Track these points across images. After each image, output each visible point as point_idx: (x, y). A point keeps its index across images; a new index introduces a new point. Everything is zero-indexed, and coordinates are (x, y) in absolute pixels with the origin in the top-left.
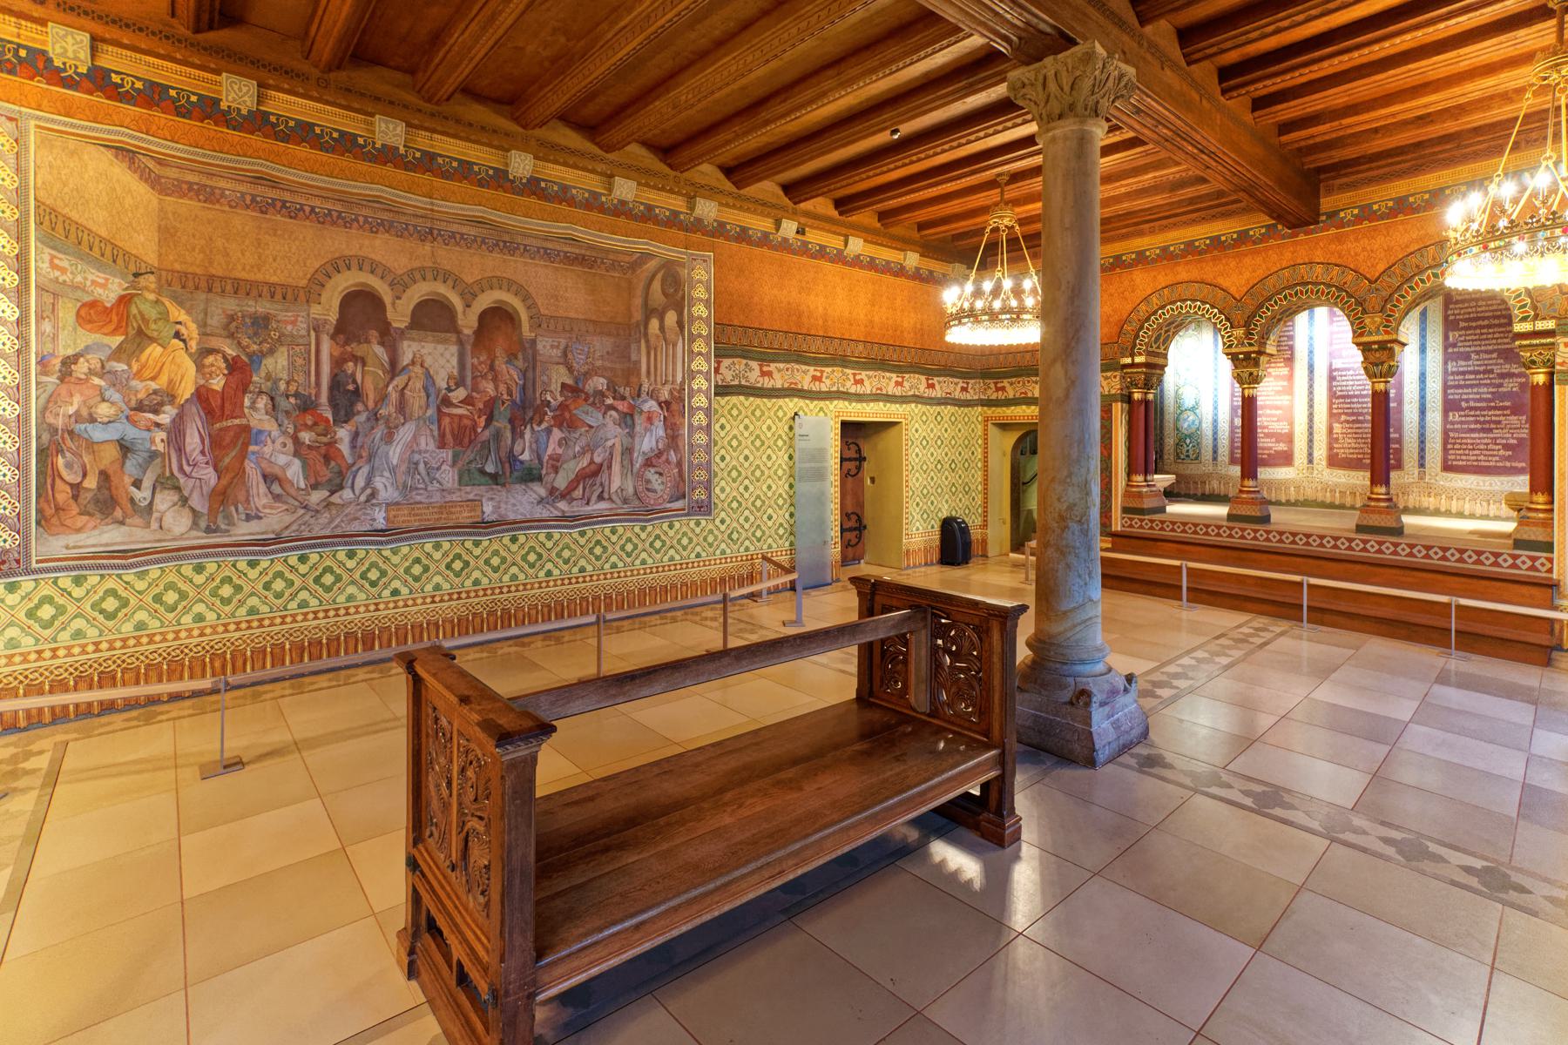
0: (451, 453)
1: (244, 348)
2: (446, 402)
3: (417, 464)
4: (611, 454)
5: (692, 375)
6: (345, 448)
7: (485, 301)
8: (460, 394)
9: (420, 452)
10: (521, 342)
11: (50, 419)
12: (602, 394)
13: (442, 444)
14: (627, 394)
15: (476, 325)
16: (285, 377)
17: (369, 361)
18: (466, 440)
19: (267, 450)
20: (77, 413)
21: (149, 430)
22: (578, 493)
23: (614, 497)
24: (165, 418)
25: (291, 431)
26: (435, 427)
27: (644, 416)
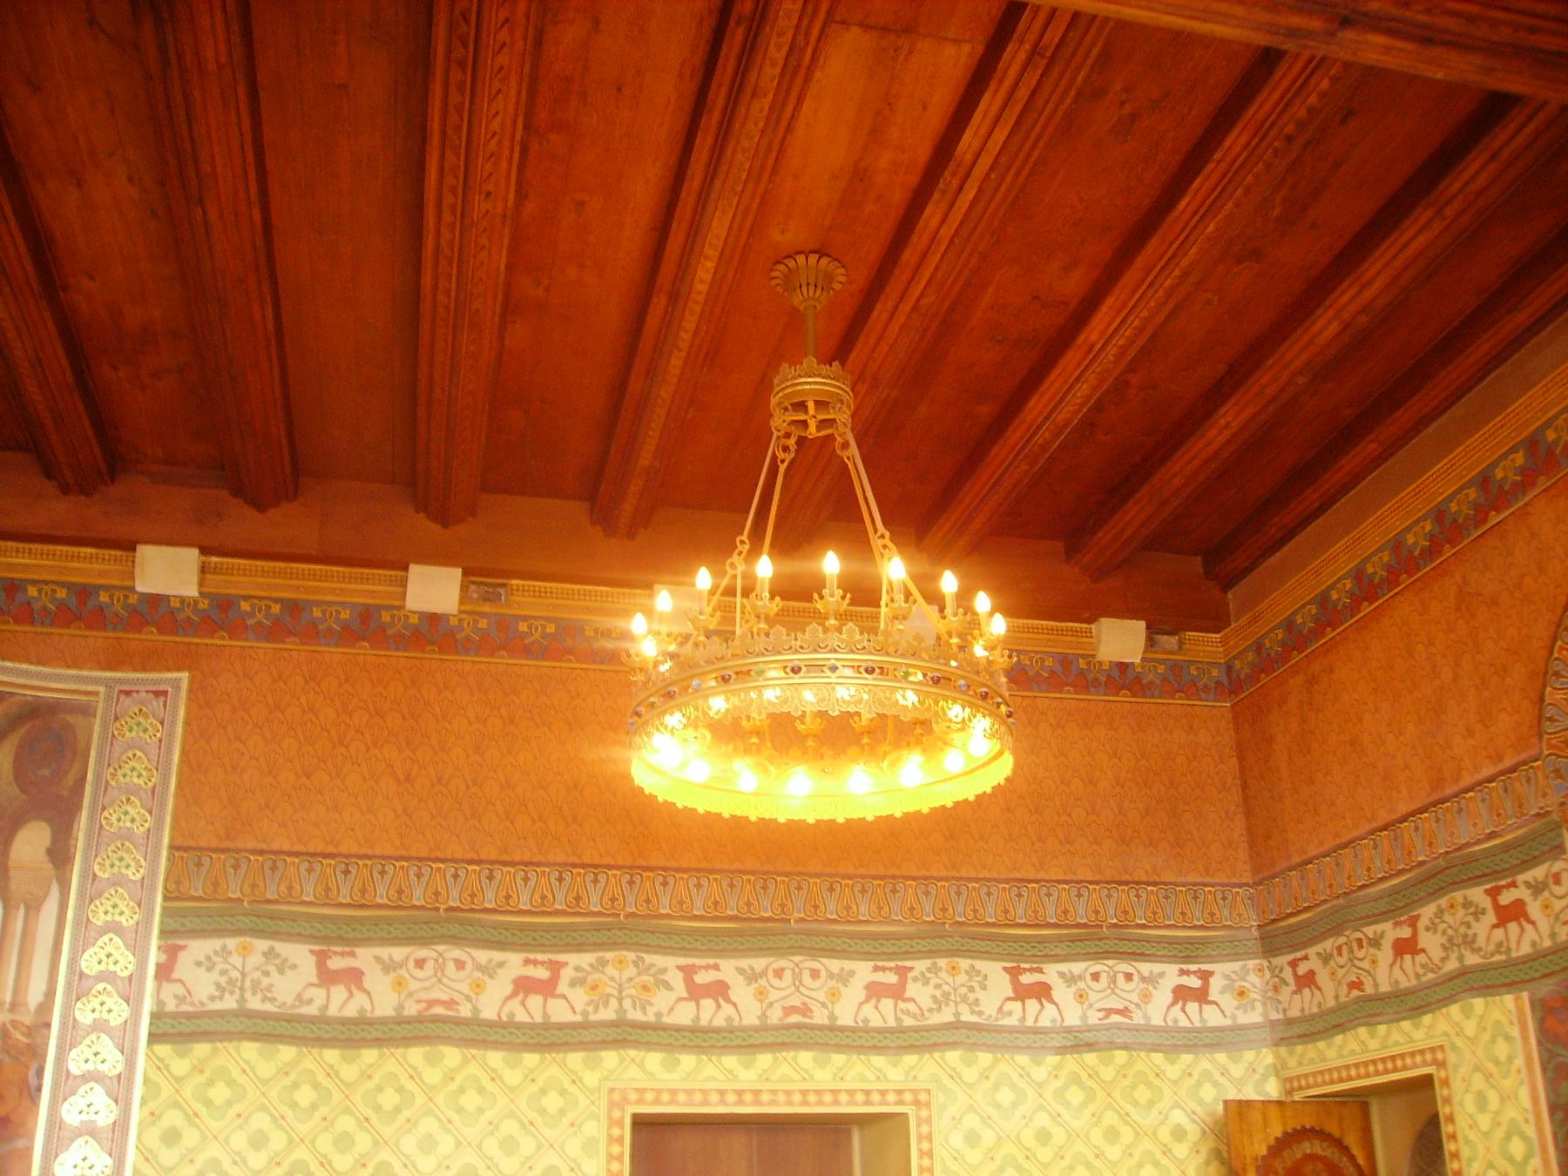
5: (80, 986)
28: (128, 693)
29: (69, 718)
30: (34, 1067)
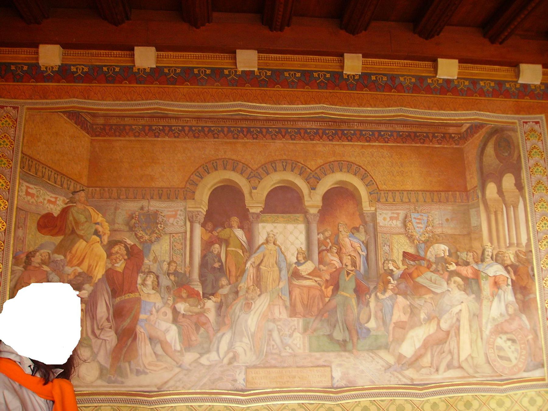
1: (139, 238)
2: (296, 275)
3: (270, 331)
4: (458, 320)
6: (212, 316)
7: (328, 183)
8: (307, 268)
9: (274, 320)
10: (362, 215)
12: (443, 261)
13: (293, 313)
14: (471, 260)
15: (320, 204)
16: (168, 259)
17: (232, 241)
18: (315, 310)
22: (426, 360)
23: (464, 365)
25: (171, 302)
26: (287, 298)
27: (491, 281)
28: (526, 123)
29: (509, 133)
30: (530, 267)
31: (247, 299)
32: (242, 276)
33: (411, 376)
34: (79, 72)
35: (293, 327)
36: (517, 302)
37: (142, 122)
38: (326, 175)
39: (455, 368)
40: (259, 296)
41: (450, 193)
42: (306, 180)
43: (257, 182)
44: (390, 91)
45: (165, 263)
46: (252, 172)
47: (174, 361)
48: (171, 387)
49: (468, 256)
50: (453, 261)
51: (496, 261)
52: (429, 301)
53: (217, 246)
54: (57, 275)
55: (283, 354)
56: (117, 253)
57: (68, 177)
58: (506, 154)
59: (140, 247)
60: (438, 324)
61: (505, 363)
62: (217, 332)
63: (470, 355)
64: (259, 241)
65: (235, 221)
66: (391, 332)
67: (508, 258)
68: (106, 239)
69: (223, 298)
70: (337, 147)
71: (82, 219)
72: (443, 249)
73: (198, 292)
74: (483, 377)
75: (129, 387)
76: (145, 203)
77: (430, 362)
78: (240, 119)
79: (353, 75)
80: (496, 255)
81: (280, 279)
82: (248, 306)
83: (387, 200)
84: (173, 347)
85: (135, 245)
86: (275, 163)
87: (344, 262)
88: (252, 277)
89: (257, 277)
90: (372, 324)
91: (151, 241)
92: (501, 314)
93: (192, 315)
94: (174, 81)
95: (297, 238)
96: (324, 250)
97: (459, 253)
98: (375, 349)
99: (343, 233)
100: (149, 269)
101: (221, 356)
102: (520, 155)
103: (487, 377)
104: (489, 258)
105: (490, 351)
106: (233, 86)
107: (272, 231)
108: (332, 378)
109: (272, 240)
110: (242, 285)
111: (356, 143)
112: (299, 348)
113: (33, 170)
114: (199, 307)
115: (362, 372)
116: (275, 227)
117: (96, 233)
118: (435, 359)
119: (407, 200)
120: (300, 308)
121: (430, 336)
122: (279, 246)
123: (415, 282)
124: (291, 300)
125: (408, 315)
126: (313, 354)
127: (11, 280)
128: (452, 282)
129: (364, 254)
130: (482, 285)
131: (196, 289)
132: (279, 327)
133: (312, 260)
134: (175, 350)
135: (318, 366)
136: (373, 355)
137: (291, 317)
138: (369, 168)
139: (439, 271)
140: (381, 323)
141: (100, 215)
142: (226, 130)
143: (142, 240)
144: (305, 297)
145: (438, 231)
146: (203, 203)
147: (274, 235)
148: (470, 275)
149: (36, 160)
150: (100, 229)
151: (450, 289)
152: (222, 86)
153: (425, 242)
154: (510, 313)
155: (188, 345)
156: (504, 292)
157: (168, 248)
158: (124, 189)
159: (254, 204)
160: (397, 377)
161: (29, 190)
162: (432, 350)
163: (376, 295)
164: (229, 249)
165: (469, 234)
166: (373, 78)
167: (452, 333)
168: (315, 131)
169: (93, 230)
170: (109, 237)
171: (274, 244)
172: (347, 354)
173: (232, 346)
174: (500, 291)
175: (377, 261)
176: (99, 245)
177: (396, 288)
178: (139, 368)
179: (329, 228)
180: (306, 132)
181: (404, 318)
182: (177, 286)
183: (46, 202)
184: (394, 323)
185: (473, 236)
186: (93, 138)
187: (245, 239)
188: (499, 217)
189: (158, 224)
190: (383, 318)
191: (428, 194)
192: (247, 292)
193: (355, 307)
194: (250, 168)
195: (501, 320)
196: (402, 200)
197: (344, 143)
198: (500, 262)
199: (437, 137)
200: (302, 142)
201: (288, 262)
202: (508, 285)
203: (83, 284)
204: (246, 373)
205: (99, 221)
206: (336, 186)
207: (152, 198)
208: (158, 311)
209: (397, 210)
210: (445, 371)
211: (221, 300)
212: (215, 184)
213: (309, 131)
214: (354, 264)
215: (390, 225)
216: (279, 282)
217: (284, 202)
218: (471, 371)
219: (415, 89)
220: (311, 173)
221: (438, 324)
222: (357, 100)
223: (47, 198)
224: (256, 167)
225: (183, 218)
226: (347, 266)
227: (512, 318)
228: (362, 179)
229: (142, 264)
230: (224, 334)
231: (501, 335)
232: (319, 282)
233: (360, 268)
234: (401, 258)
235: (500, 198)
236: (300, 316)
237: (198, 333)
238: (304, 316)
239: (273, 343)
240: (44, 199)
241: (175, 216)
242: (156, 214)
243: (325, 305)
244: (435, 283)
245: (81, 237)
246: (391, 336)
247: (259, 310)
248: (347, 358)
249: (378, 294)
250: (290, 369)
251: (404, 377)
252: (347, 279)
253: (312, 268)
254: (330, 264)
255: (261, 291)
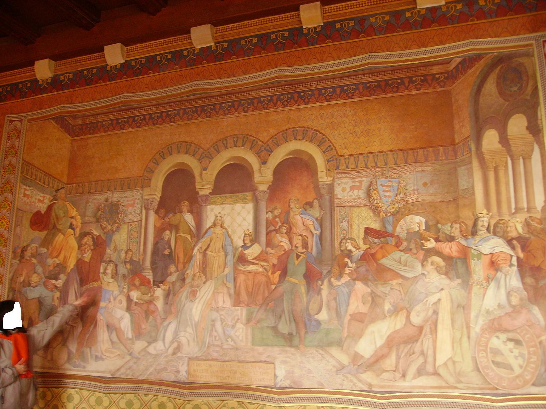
0: (245, 311)
1: (103, 229)
2: (242, 259)
4: (436, 312)
6: (160, 304)
7: (280, 155)
9: (217, 310)
10: (317, 188)
11: (13, 286)
12: (418, 238)
13: (237, 302)
14: (456, 233)
15: (271, 179)
18: (260, 298)
19: (110, 306)
20: (24, 281)
21: (52, 291)
22: (390, 362)
23: (441, 371)
24: (59, 283)
25: (125, 290)
26: (231, 285)
29: (520, 60)
31: (192, 286)
32: (189, 263)
33: (369, 380)
34: (66, 80)
35: (237, 318)
36: (526, 289)
37: (111, 117)
38: (278, 146)
39: (428, 374)
40: (204, 283)
41: (431, 149)
42: (257, 154)
43: (208, 162)
44: (358, 37)
45: (123, 252)
46: (203, 153)
47: (126, 348)
48: (122, 374)
49: (454, 229)
50: (432, 235)
51: (495, 234)
52: (397, 288)
53: (168, 232)
54: (41, 266)
55: (225, 346)
56: (86, 244)
57: (53, 177)
58: (515, 89)
59: (103, 237)
60: (408, 317)
61: (503, 372)
62: (164, 321)
63: (451, 358)
64: (206, 224)
65: (185, 204)
66: (346, 326)
67: (513, 228)
68: (78, 231)
69: (171, 286)
70: (292, 113)
71: (61, 213)
72: (418, 221)
73: (149, 279)
74: (468, 388)
75: (89, 371)
76: (109, 195)
77: (394, 365)
78: (195, 99)
79: (315, 28)
80: (495, 226)
81: (226, 264)
82: (194, 294)
83: (347, 167)
84: (126, 335)
85: (100, 235)
86: (226, 140)
87: (294, 243)
88: (198, 263)
89: (203, 263)
90: (323, 316)
91: (112, 230)
92: (499, 306)
93: (143, 303)
94: (140, 73)
95: (244, 219)
96: (272, 231)
97: (440, 226)
98: (325, 345)
99: (295, 210)
100: (110, 258)
101: (167, 346)
102: (537, 87)
103: (474, 388)
104: (484, 229)
105: (481, 355)
106: (191, 66)
107: (220, 213)
108: (275, 376)
109: (220, 222)
110: (188, 272)
111: (314, 105)
112: (242, 341)
113: (30, 174)
114: (149, 295)
115: (310, 372)
116: (223, 209)
117: (71, 226)
118: (401, 361)
119: (373, 165)
120: (244, 296)
121: (396, 332)
122: (226, 229)
123: (378, 264)
124: (235, 287)
125: (368, 305)
126: (256, 348)
127: (10, 272)
128: (429, 264)
129: (318, 232)
130: (472, 266)
131: (148, 277)
132: (222, 317)
133: (259, 243)
134: (127, 338)
135: (260, 362)
136: (322, 352)
137: (234, 306)
138: (327, 132)
139: (411, 250)
140: (334, 315)
141: (75, 209)
142: (181, 112)
143: (105, 230)
144: (250, 283)
145: (412, 199)
146: (158, 189)
147: (222, 217)
148: (455, 254)
149: (32, 165)
150: (74, 223)
151: (426, 273)
152: (180, 68)
153: (394, 214)
154: (513, 303)
155: (138, 333)
156: (506, 276)
157: (126, 237)
158: (93, 183)
159: (204, 186)
160: (351, 381)
161: (27, 193)
162: (398, 349)
163: (329, 281)
164: (178, 235)
165: (455, 200)
166: (338, 26)
167: (427, 329)
168: (269, 98)
169: (69, 224)
170: (80, 229)
171: (222, 227)
172: (292, 350)
173: (177, 335)
174: (499, 274)
175: (332, 240)
176: (72, 237)
177: (354, 272)
178: (97, 354)
179: (278, 205)
180: (260, 102)
181: (364, 309)
182: (132, 274)
183: (37, 201)
184: (350, 315)
185: (461, 202)
186: (73, 139)
187: (193, 223)
188: (501, 173)
189: (119, 214)
190: (336, 309)
191: (400, 153)
192: (193, 279)
193: (304, 296)
194: (202, 148)
195: (499, 313)
196: (366, 165)
197: (300, 107)
198: (501, 234)
199: (415, 81)
200: (254, 113)
201: (235, 245)
202: (511, 265)
203: (59, 274)
204: (188, 365)
205: (73, 215)
206: (288, 157)
207: (115, 189)
208: (115, 299)
209: (360, 177)
210: (414, 378)
211: (169, 288)
212: (169, 169)
213: (262, 99)
214: (305, 245)
215: (351, 196)
216: (225, 267)
217: (234, 180)
218: (452, 380)
219: (389, 28)
220: (263, 146)
221: (408, 317)
222: (318, 55)
223: (39, 197)
224: (208, 146)
225: (139, 206)
226: (297, 247)
227: (516, 310)
228: (319, 146)
229: (105, 254)
230: (170, 323)
231: (498, 334)
232: (266, 267)
233: (312, 250)
234: (362, 235)
235: (504, 149)
236: (243, 305)
237: (147, 322)
238: (248, 305)
239: (215, 334)
240: (36, 199)
241: (133, 205)
242: (117, 205)
243: (272, 292)
244: (406, 265)
245: (60, 231)
246: (346, 330)
247: (204, 298)
248: (293, 354)
249: (332, 280)
250: (231, 363)
251: (360, 381)
252: (297, 262)
253: (259, 252)
254: (278, 246)
255: (206, 277)
